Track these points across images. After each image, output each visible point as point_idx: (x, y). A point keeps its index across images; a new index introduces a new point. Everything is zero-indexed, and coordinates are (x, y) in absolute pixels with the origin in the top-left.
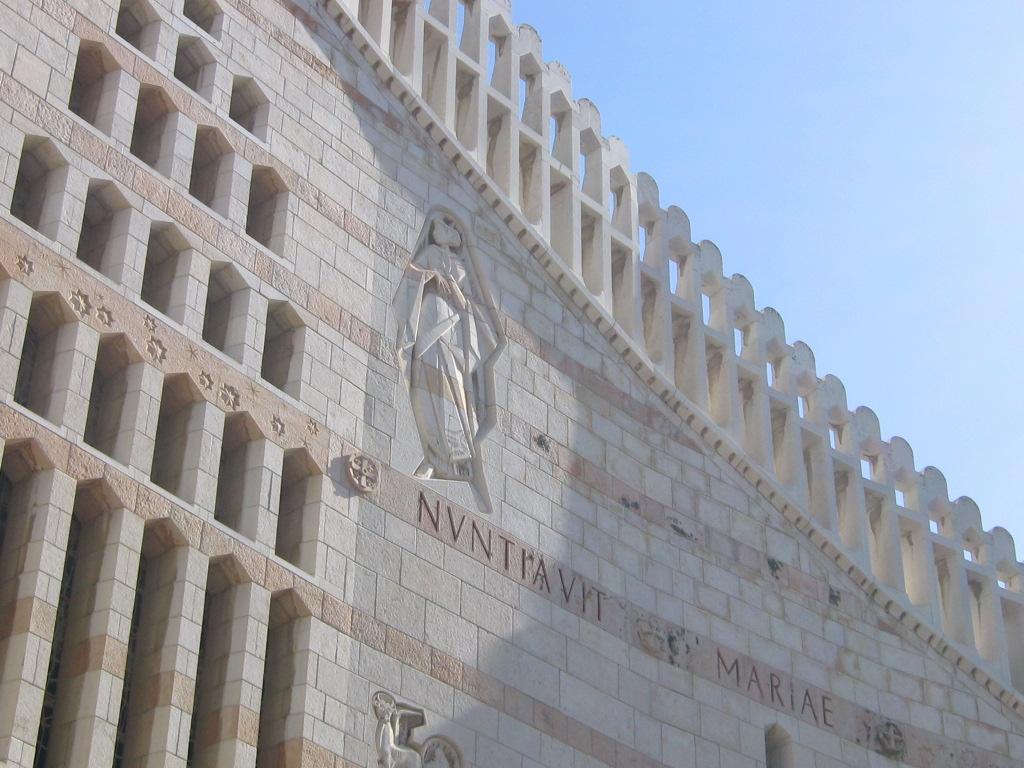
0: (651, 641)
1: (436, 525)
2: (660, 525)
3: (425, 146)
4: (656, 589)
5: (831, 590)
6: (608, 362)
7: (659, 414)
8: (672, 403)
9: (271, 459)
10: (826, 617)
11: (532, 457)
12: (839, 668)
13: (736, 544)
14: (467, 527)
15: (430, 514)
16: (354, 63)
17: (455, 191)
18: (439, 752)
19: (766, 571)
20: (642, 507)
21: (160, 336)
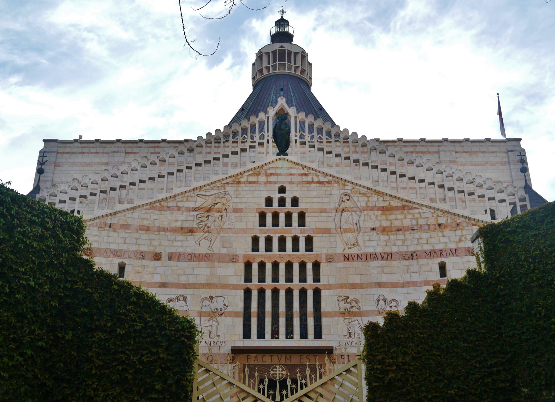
0: (406, 258)
1: (348, 260)
2: (408, 231)
3: (338, 182)
4: (407, 246)
5: (457, 223)
6: (391, 201)
7: (406, 206)
8: (409, 202)
9: (309, 266)
10: (456, 230)
11: (371, 234)
12: (460, 240)
13: (429, 225)
14: (356, 256)
15: (347, 258)
16: (319, 176)
17: (347, 187)
18: (354, 302)
19: (438, 227)
20: (403, 229)
21: (283, 256)
